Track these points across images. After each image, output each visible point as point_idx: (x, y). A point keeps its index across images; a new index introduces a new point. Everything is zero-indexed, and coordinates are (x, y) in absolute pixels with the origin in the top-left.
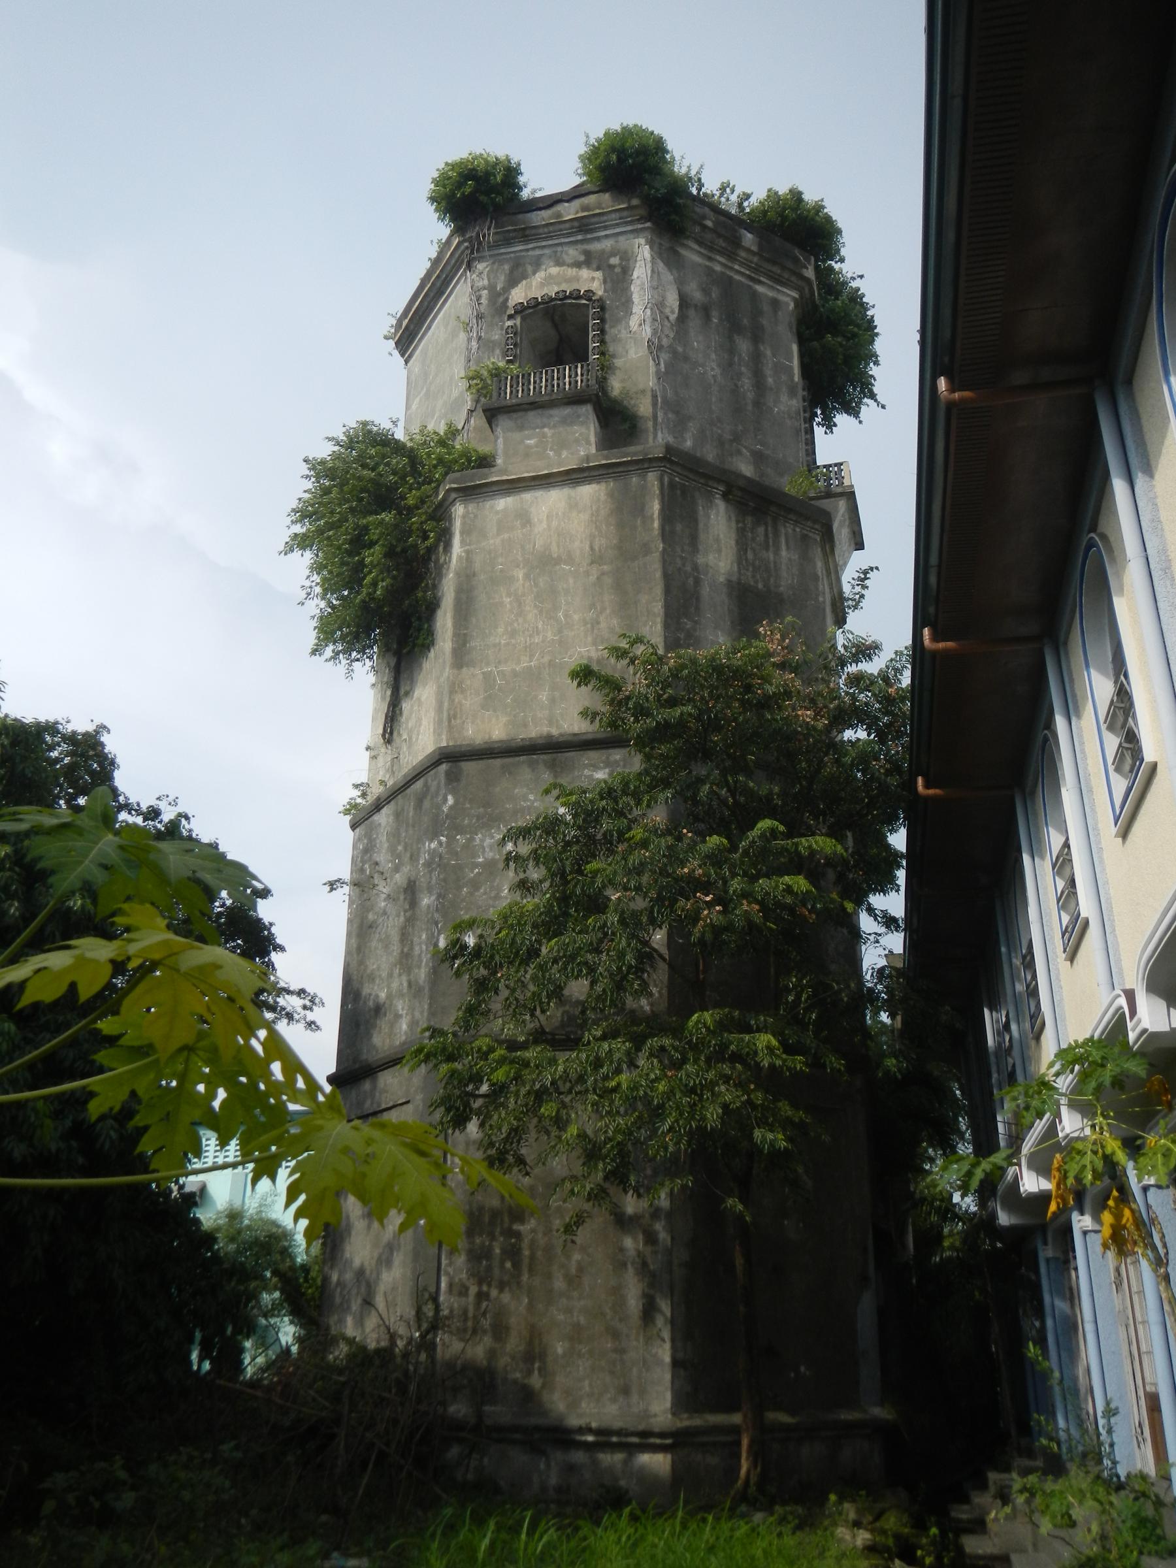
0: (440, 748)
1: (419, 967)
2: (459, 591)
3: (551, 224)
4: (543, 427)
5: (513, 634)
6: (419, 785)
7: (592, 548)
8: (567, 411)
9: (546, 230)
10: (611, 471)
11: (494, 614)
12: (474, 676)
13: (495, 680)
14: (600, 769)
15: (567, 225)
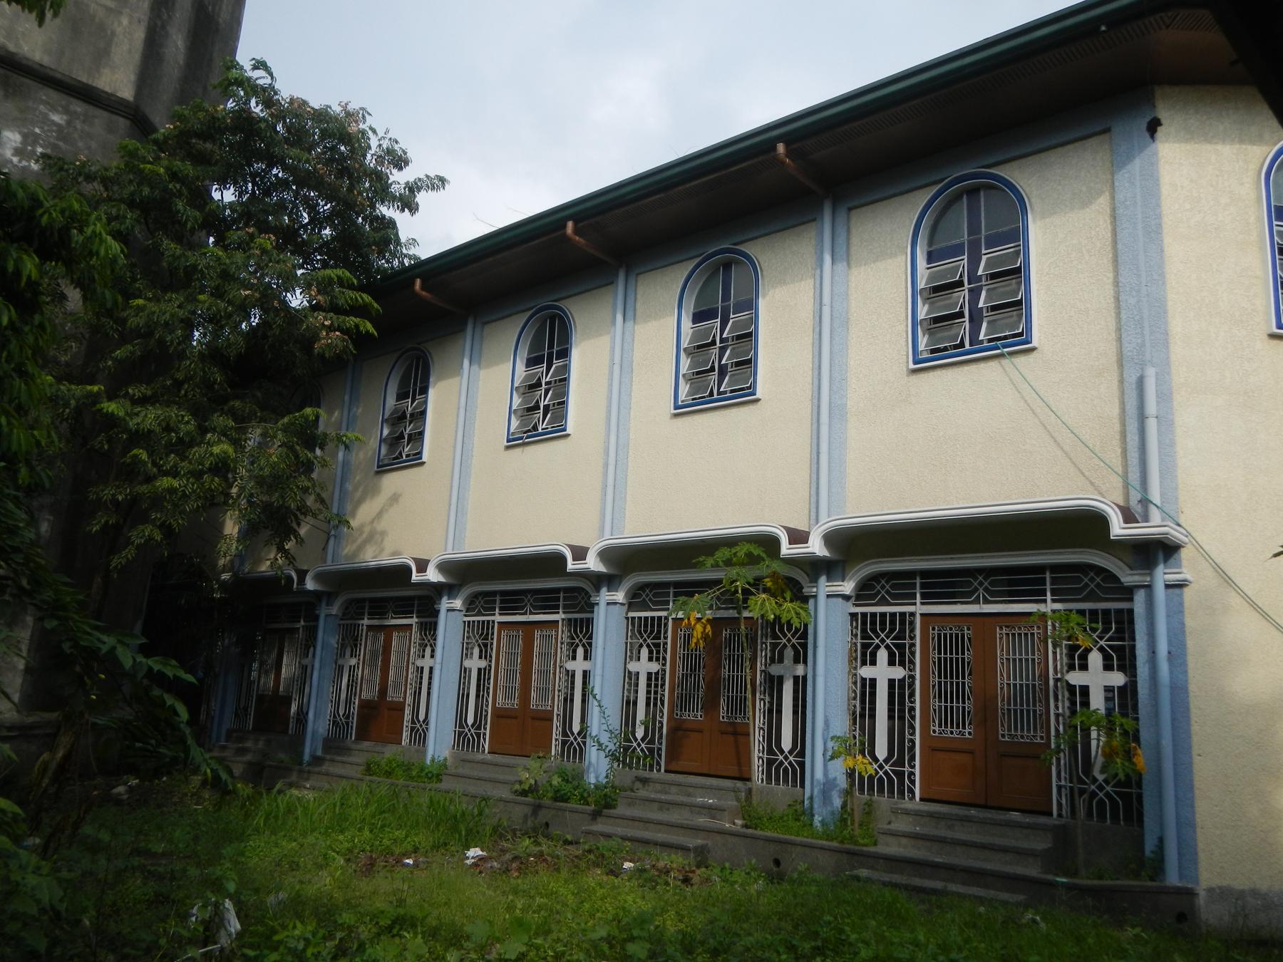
14: (57, 112)
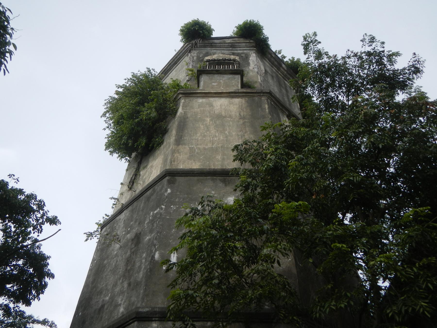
0: (166, 169)
1: (138, 272)
2: (180, 122)
3: (222, 43)
4: (220, 80)
5: (205, 136)
6: (148, 193)
7: (240, 115)
8: (231, 76)
9: (219, 45)
10: (247, 95)
11: (196, 130)
12: (185, 148)
13: (195, 150)
15: (227, 44)
